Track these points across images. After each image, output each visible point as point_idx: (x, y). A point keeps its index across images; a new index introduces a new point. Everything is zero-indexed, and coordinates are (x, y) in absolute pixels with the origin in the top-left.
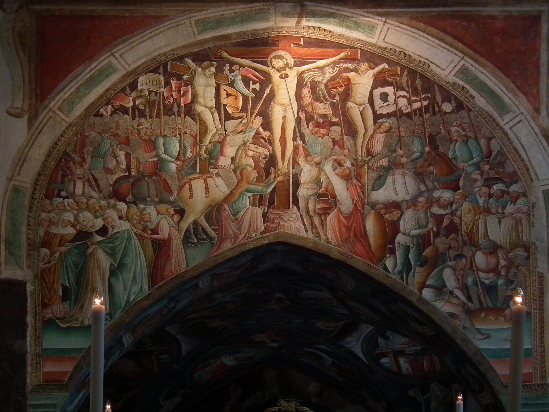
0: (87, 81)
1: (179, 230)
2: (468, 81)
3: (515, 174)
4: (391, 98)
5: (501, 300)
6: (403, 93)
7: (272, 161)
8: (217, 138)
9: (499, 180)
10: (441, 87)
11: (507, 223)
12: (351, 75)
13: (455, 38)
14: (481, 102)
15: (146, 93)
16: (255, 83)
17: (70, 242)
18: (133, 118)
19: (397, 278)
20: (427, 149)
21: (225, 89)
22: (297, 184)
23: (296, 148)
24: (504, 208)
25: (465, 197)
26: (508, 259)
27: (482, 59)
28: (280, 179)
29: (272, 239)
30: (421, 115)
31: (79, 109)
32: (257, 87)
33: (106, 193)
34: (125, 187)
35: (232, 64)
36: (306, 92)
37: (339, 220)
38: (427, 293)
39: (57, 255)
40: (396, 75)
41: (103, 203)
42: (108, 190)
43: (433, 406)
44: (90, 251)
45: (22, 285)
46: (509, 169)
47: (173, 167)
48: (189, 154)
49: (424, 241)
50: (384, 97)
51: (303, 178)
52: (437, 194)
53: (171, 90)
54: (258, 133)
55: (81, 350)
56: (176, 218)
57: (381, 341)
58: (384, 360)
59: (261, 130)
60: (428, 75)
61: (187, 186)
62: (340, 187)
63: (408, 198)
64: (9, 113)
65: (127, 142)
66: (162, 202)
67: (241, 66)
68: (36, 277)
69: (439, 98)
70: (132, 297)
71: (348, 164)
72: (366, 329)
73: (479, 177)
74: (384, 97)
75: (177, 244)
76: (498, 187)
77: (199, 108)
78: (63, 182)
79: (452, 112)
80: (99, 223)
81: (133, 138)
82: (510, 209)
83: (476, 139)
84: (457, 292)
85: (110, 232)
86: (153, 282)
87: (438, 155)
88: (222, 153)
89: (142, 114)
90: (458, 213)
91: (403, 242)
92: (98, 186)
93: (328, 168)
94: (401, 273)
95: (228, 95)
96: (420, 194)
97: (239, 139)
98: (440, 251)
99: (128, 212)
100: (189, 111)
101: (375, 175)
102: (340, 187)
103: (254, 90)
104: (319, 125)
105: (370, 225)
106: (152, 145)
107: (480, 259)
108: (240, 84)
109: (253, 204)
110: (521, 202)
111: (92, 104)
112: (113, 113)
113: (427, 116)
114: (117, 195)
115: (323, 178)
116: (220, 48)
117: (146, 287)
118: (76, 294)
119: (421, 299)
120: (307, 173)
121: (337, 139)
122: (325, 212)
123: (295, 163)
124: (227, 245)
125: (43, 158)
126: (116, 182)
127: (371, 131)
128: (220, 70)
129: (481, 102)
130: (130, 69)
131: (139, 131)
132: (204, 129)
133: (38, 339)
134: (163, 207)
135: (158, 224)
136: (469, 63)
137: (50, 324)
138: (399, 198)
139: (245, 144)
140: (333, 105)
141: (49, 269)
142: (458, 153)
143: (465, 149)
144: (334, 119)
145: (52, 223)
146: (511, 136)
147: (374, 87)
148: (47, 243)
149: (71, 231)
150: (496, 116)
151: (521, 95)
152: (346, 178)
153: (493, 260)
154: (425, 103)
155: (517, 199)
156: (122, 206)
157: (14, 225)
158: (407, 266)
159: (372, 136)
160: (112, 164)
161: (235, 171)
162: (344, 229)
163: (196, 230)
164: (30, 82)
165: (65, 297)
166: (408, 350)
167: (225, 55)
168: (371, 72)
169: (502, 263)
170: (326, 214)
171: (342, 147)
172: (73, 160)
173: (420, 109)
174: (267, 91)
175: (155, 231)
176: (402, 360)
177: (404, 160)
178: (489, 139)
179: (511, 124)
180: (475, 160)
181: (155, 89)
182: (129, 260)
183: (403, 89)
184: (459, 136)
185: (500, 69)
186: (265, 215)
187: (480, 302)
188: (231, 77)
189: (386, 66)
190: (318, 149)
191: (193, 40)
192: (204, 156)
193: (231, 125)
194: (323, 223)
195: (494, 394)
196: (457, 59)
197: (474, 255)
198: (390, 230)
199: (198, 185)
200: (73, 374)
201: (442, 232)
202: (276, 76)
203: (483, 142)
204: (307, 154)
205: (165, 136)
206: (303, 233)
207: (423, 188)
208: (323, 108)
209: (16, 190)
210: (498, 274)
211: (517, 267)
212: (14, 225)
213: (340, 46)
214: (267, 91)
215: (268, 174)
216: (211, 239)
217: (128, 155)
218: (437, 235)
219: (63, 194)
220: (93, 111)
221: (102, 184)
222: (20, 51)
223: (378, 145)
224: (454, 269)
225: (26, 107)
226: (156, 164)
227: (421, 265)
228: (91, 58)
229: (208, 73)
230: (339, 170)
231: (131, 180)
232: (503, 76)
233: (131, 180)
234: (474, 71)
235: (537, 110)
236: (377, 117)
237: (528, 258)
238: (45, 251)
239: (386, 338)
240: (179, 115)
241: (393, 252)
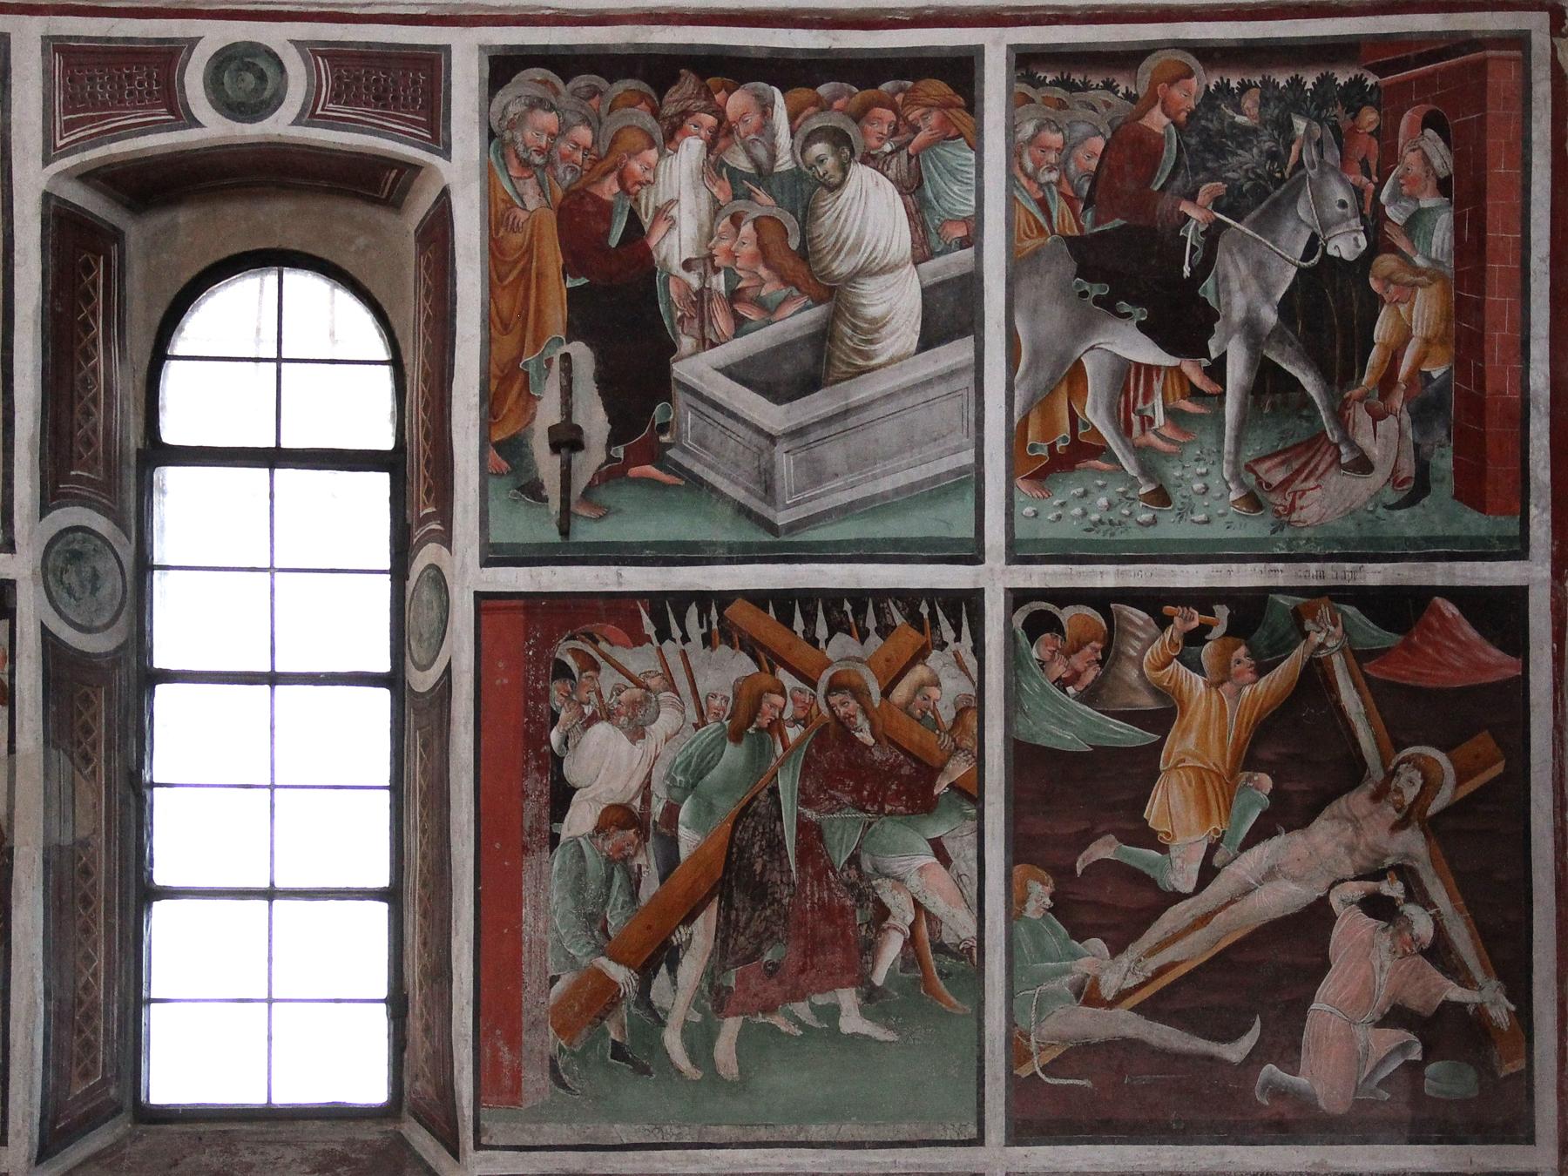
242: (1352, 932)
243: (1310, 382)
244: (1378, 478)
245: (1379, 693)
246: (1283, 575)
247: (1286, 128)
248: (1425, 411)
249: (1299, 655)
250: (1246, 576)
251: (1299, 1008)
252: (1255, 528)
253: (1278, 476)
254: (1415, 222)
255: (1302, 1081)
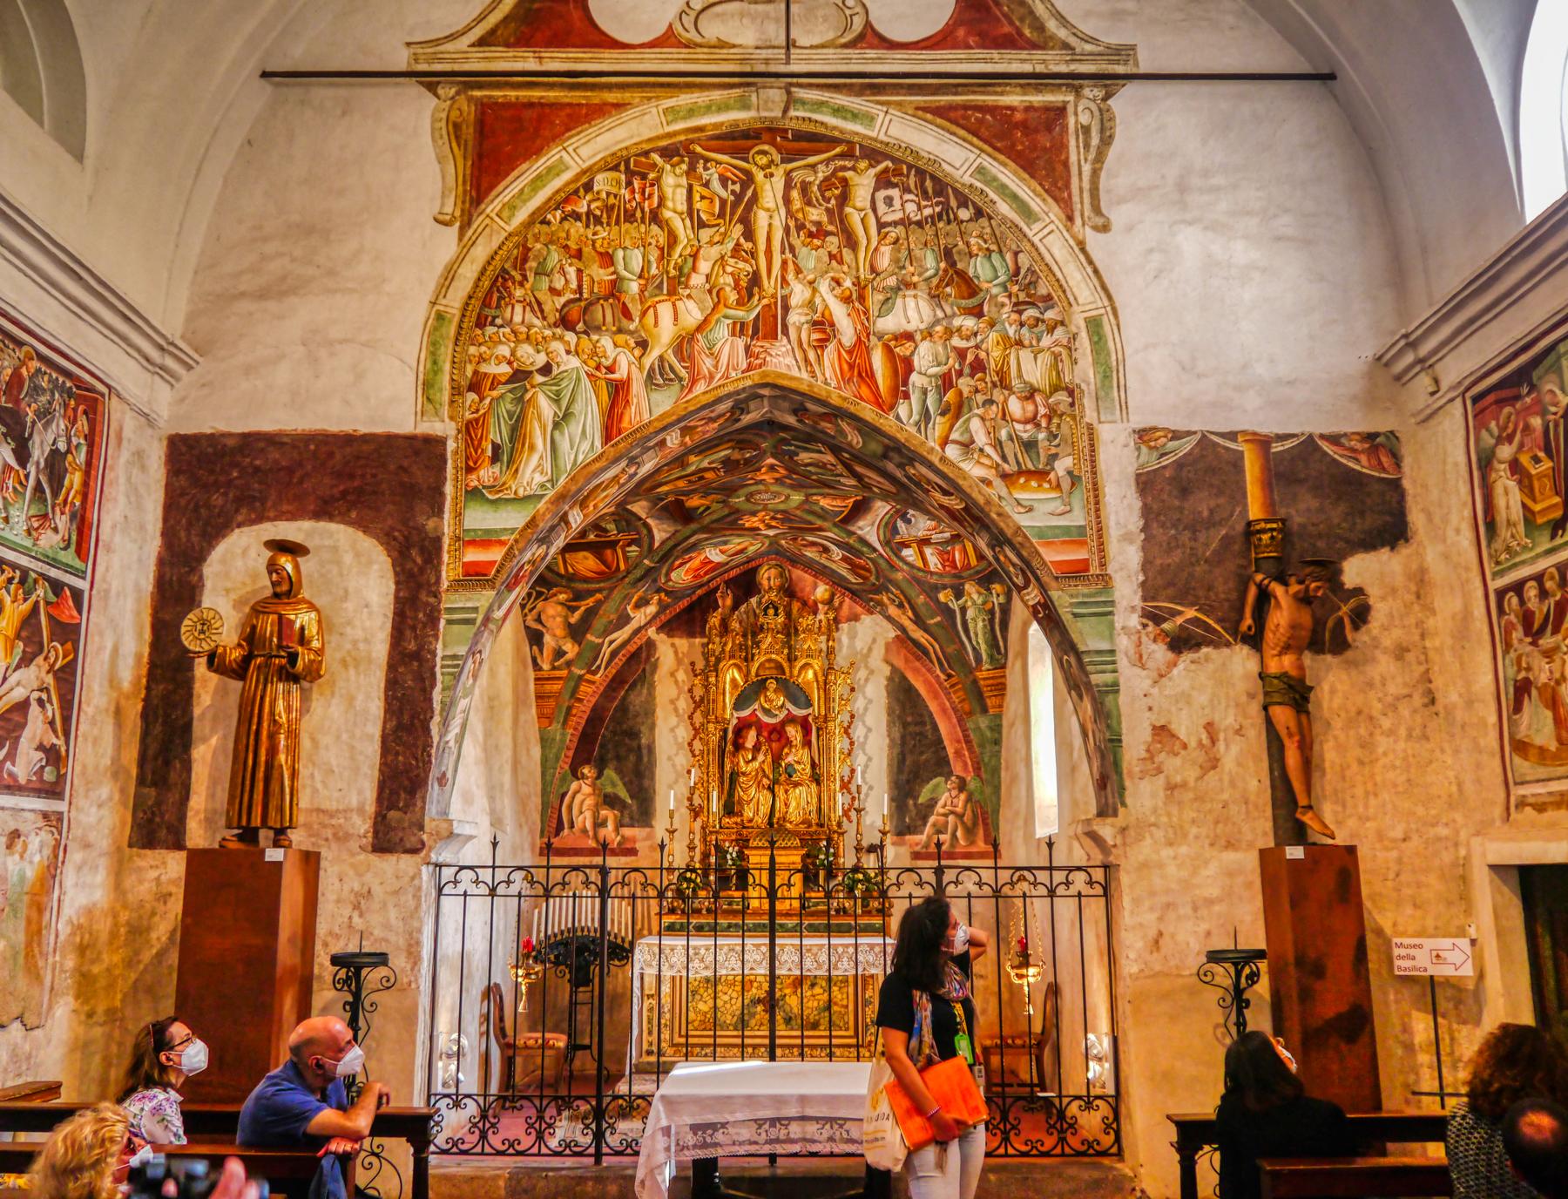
0: (533, 181)
1: (641, 368)
2: (987, 183)
3: (1049, 298)
4: (897, 203)
5: (1043, 459)
6: (911, 197)
7: (755, 280)
8: (688, 250)
9: (1033, 304)
10: (955, 190)
11: (1044, 358)
12: (848, 174)
13: (969, 131)
14: (1004, 208)
15: (604, 195)
16: (734, 183)
17: (506, 383)
18: (588, 226)
19: (913, 430)
20: (943, 265)
21: (697, 188)
22: (786, 308)
23: (784, 263)
24: (1039, 340)
25: (992, 325)
26: (1048, 406)
27: (1002, 157)
28: (765, 301)
29: (757, 380)
30: (934, 224)
31: (522, 215)
32: (737, 188)
33: (551, 320)
34: (575, 310)
35: (707, 160)
36: (795, 194)
37: (839, 354)
38: (952, 452)
39: (487, 401)
40: (901, 174)
41: (548, 333)
42: (553, 317)
43: (970, 614)
44: (528, 396)
45: (441, 442)
46: (1042, 290)
47: (634, 287)
48: (654, 271)
49: (946, 382)
50: (889, 201)
51: (793, 302)
52: (957, 322)
53: (633, 192)
54: (738, 244)
55: (513, 530)
56: (637, 352)
57: (900, 524)
58: (906, 552)
59: (742, 240)
60: (939, 174)
61: (651, 311)
62: (840, 314)
63: (922, 326)
64: (436, 220)
65: (579, 255)
66: (620, 331)
67: (718, 163)
68: (459, 431)
69: (953, 203)
70: (581, 457)
71: (848, 283)
72: (881, 508)
73: (1006, 301)
74: (889, 201)
75: (637, 387)
76: (1031, 312)
77: (667, 214)
78: (498, 306)
79: (971, 220)
80: (541, 360)
81: (587, 250)
82: (1046, 341)
83: (1000, 251)
84: (989, 450)
85: (555, 371)
86: (608, 435)
87: (958, 272)
88: (694, 269)
89: (598, 221)
90: (984, 346)
91: (918, 384)
92: (542, 311)
93: (824, 287)
94: (917, 424)
95: (703, 198)
96: (937, 322)
97: (715, 252)
98: (965, 394)
99: (577, 345)
100: (655, 217)
101: (881, 297)
102: (840, 314)
103: (733, 192)
104: (811, 235)
105: (878, 361)
106: (607, 259)
107: (1015, 406)
108: (716, 184)
109: (734, 334)
110: (1059, 331)
111: (539, 209)
112: (563, 219)
113: (941, 225)
114: (566, 322)
115: (818, 300)
116: (692, 141)
117: (598, 443)
118: (507, 454)
119: (943, 459)
120: (799, 293)
121: (835, 251)
122: (821, 345)
123: (784, 281)
124: (701, 387)
125: (475, 275)
126: (564, 305)
127: (874, 243)
128: (692, 168)
129: (1004, 208)
130: (585, 166)
131: (594, 242)
132: (673, 239)
133: (458, 515)
134: (621, 338)
135: (615, 361)
136: (986, 162)
137: (474, 494)
138: (910, 328)
139: (722, 257)
140: (827, 210)
141: (477, 420)
142: (979, 270)
143: (987, 265)
144: (830, 228)
145: (482, 359)
146: (1042, 250)
147: (876, 189)
148: (474, 387)
149: (505, 369)
150: (1022, 225)
151: (1050, 200)
152: (847, 300)
153: (1030, 408)
154: (938, 209)
155: (1054, 328)
156: (570, 337)
157: (435, 363)
158: (926, 415)
159: (876, 249)
160: (559, 283)
161: (710, 291)
162: (845, 367)
163: (661, 367)
164: (464, 182)
165: (495, 458)
166: (936, 538)
167: (699, 149)
168: (873, 172)
169: (1042, 411)
170: (823, 348)
171: (841, 262)
172: (512, 278)
173: (932, 217)
174: (749, 193)
175: (611, 370)
176: (928, 551)
177: (915, 279)
178: (1016, 254)
179: (1041, 235)
180: (1002, 279)
181: (614, 190)
182: (577, 408)
183: (910, 192)
184: (980, 249)
185: (1025, 169)
186: (747, 348)
187: (1018, 463)
188: (705, 176)
189: (889, 164)
190: (811, 264)
191: (661, 132)
192: (673, 273)
193: (705, 234)
194: (819, 359)
195: (1043, 589)
196: (973, 157)
197: (1006, 401)
198: (902, 368)
199: (665, 310)
200: (502, 565)
201: (967, 370)
202: (759, 176)
203: (1008, 257)
204: (798, 271)
205: (625, 248)
206: (795, 373)
207: (940, 314)
208: (816, 214)
209: (440, 317)
210: (1038, 425)
211: (1061, 416)
212: (435, 363)
213: (835, 141)
214: (749, 193)
215: (751, 296)
216: (681, 379)
217: (579, 271)
218: (960, 374)
219: (499, 321)
220: (539, 218)
221: (547, 308)
222: (454, 145)
223: (884, 262)
224: (983, 419)
225: (458, 213)
226: (613, 283)
227: (943, 414)
228: (538, 152)
229: (678, 171)
230: (838, 291)
231: (583, 304)
232: (1026, 176)
233: (583, 304)
234: (994, 171)
235: (1070, 218)
236: (881, 226)
237: (1072, 405)
238: (472, 396)
239: (908, 522)
240: (643, 222)
241: (907, 396)
242: (34, 708)
243: (48, 491)
244: (59, 537)
245: (50, 617)
246: (34, 565)
247: (53, 394)
248: (73, 517)
249: (33, 598)
250: (24, 561)
251: (18, 738)
252: (28, 543)
253: (36, 525)
254: (78, 446)
255: (15, 770)
